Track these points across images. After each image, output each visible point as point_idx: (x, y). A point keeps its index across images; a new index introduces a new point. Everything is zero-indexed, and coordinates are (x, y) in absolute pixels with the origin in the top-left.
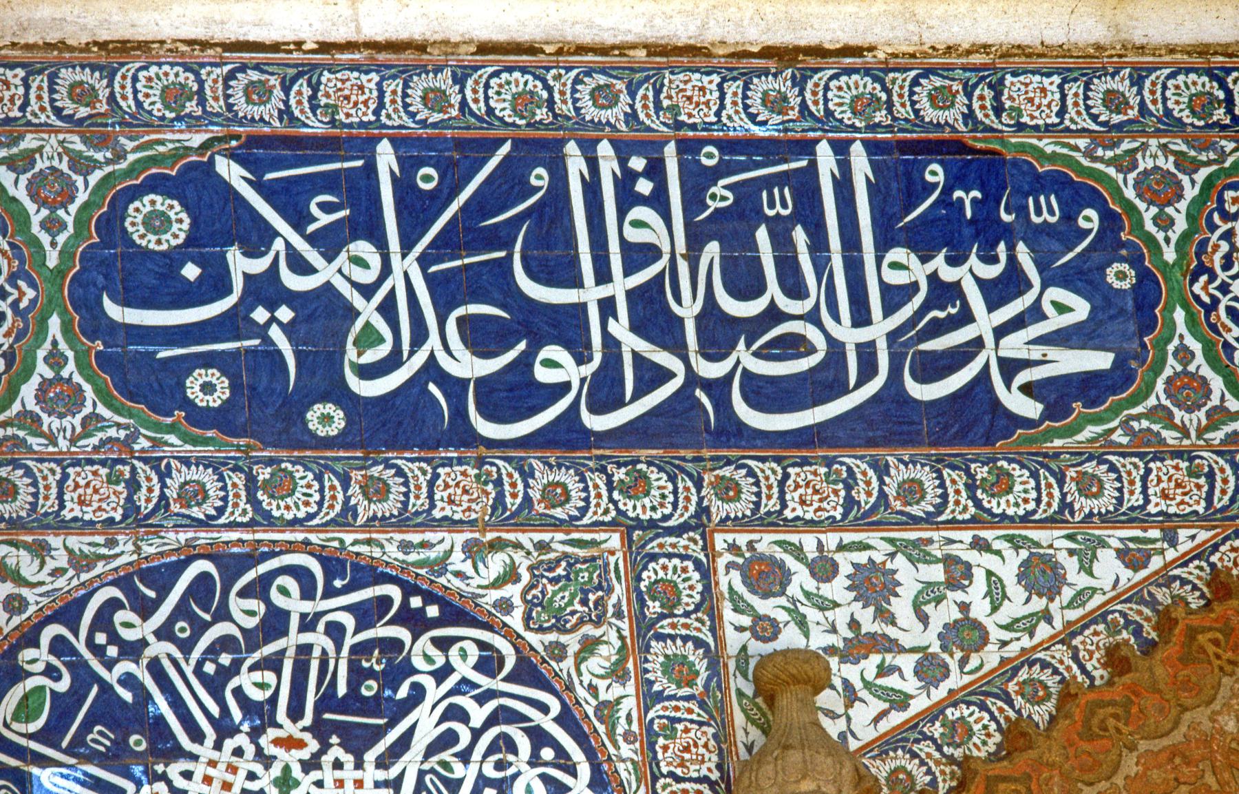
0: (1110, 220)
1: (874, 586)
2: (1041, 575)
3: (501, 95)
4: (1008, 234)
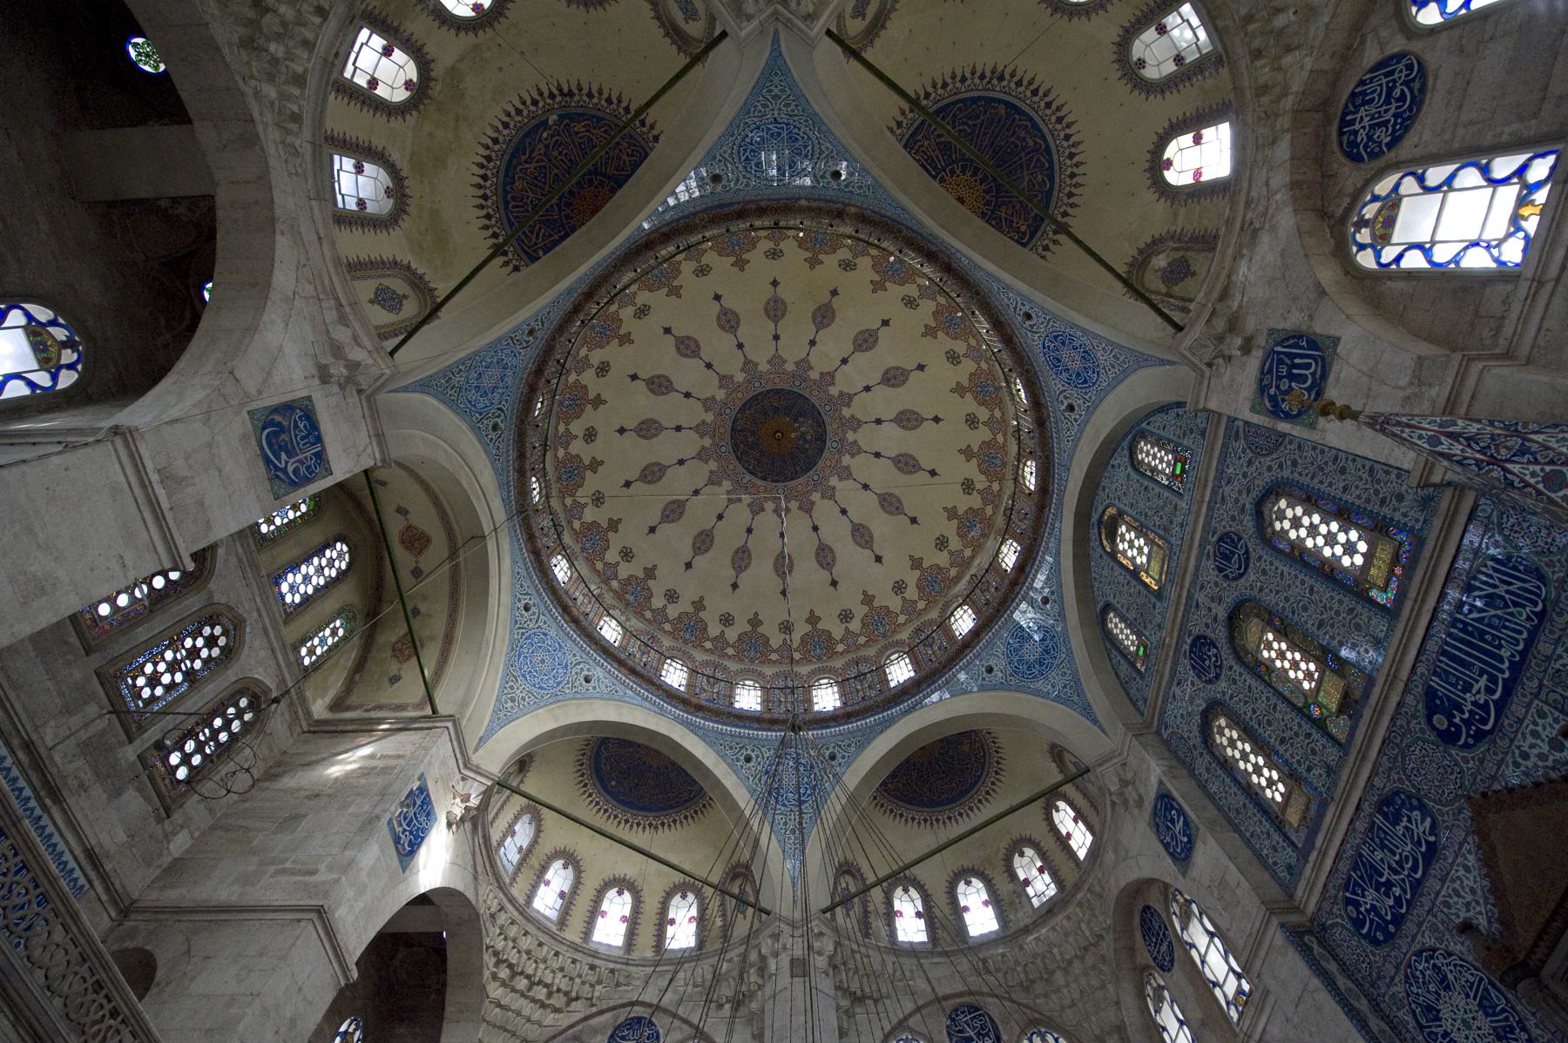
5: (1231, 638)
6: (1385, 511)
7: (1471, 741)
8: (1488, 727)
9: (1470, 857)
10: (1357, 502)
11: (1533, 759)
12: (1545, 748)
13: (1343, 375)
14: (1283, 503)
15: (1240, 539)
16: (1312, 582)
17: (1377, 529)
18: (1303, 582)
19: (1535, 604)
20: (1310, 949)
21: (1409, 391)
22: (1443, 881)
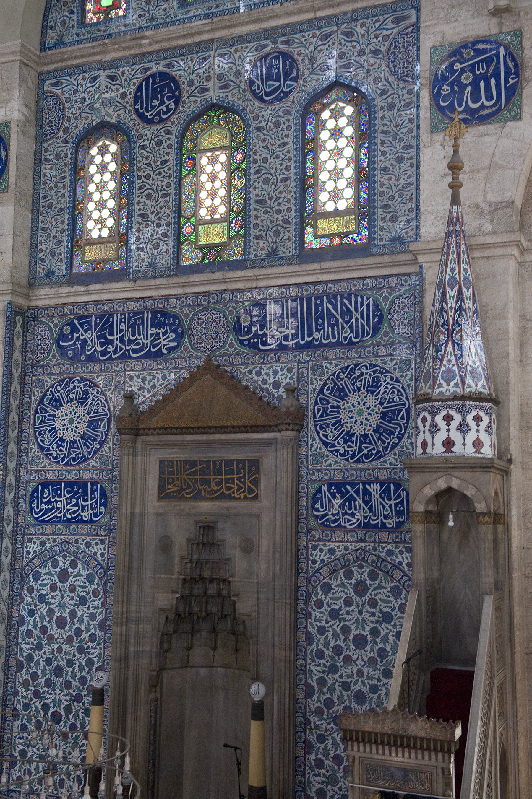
0: (180, 321)
1: (144, 380)
2: (164, 377)
3: (107, 307)
4: (167, 325)
5: (195, 118)
6: (379, 212)
7: (246, 343)
8: (262, 347)
9: (173, 376)
10: (377, 185)
11: (260, 378)
12: (271, 380)
13: (487, 139)
14: (349, 110)
15: (295, 79)
16: (293, 177)
17: (364, 211)
18: (288, 168)
19: (356, 337)
20: (15, 326)
21: (483, 205)
22: (144, 369)
